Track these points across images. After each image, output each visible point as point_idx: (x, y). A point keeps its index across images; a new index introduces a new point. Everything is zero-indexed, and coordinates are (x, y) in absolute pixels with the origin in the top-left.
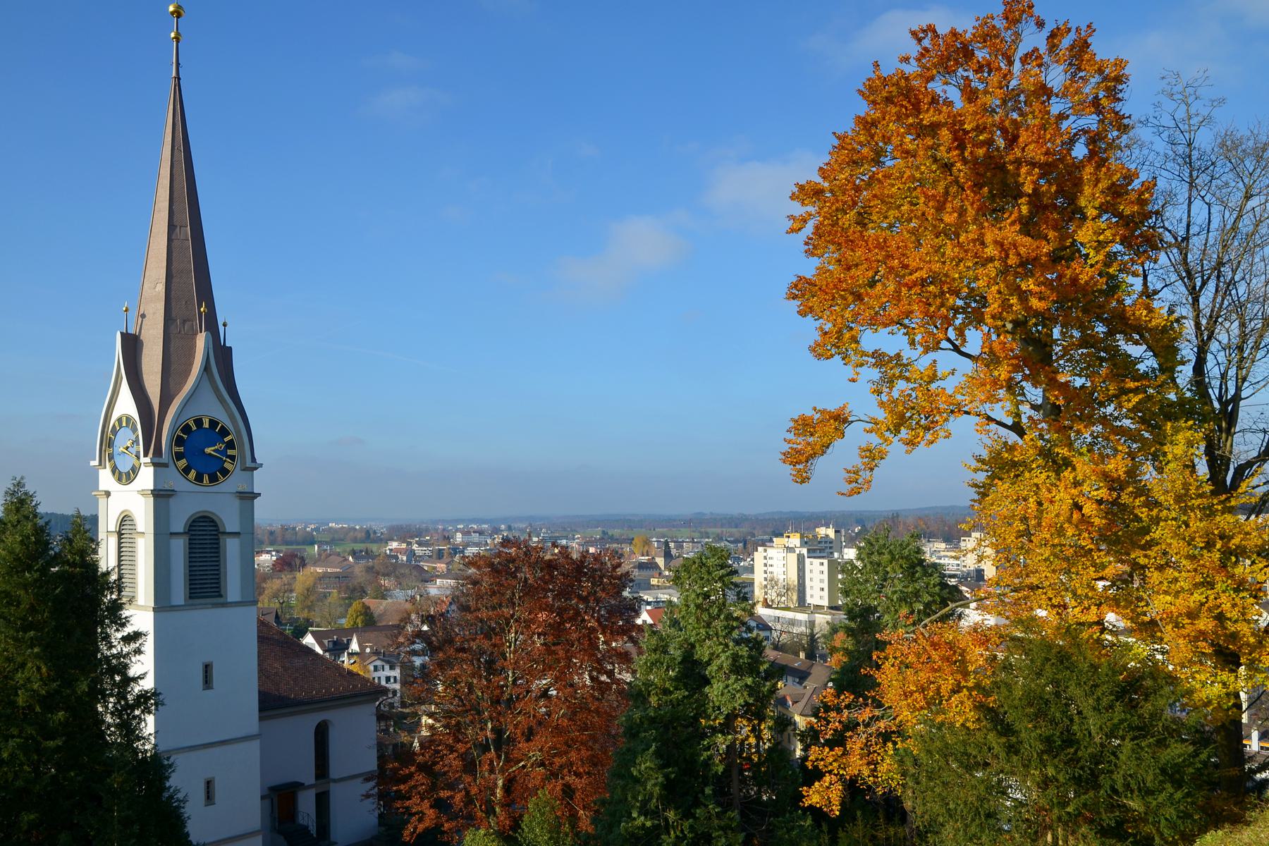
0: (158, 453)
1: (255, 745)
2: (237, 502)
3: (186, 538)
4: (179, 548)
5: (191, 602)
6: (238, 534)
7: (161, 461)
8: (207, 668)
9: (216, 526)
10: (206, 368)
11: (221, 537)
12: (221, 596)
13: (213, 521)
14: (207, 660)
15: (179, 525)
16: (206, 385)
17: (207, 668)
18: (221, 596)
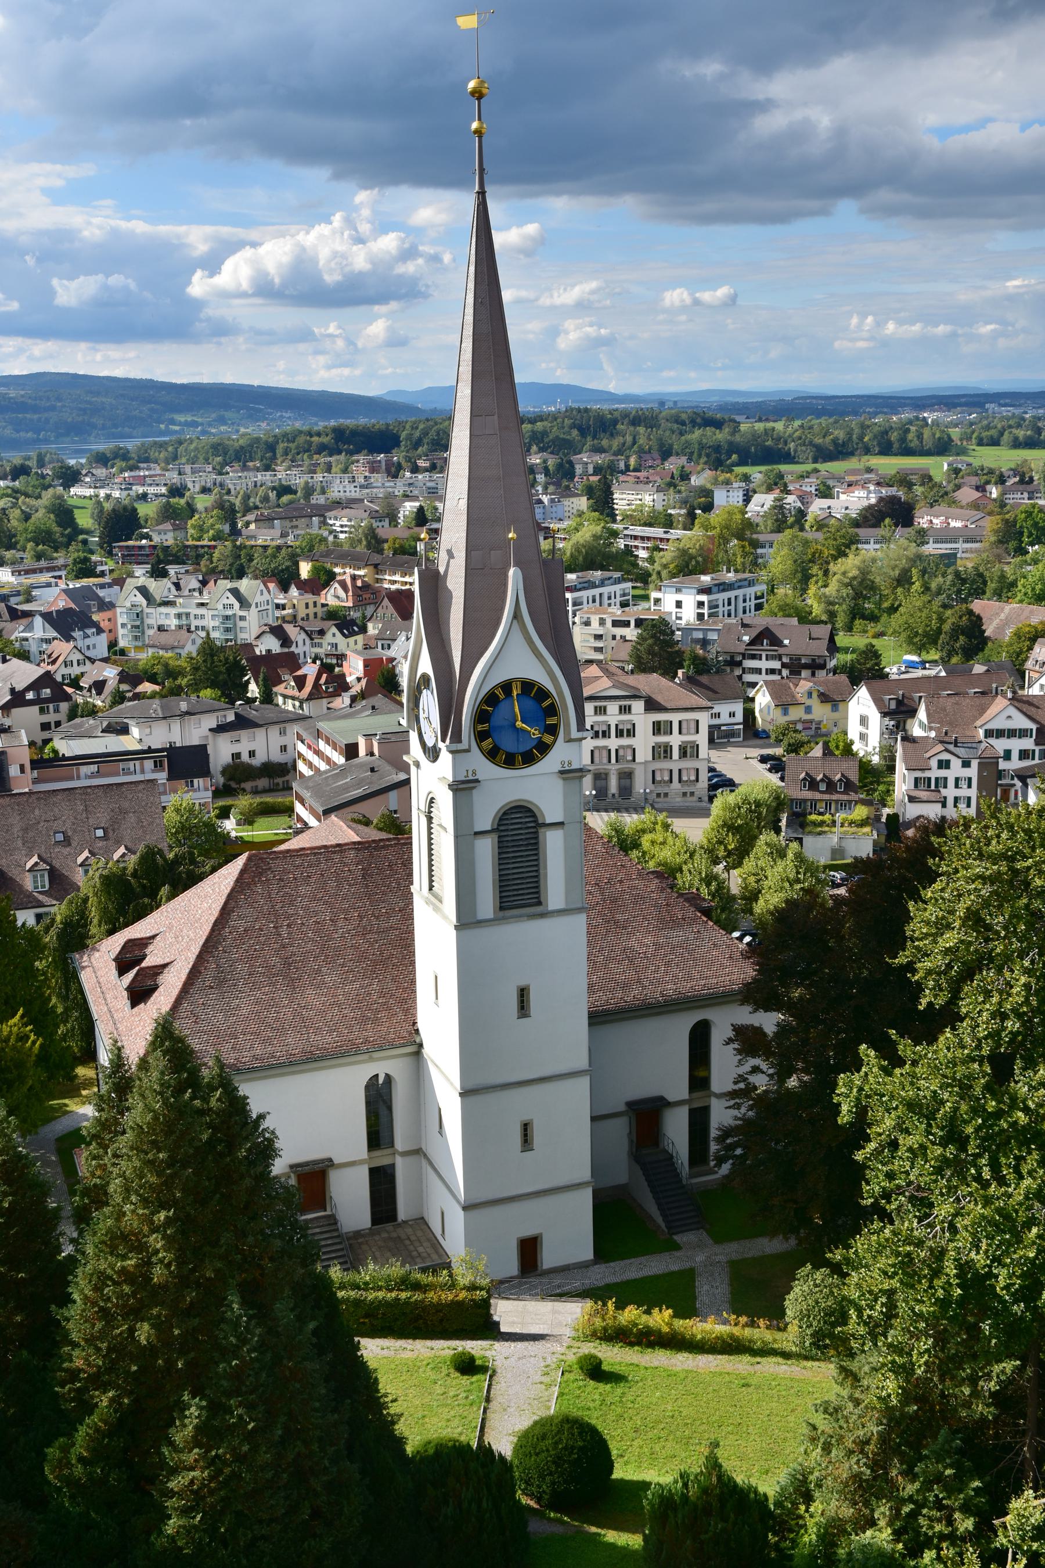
0: (457, 738)
1: (585, 1082)
2: (559, 783)
3: (495, 837)
4: (486, 850)
5: (501, 914)
6: (561, 824)
7: (460, 747)
8: (523, 993)
9: (534, 816)
10: (516, 615)
11: (541, 830)
12: (539, 903)
13: (530, 810)
14: (523, 983)
15: (485, 820)
16: (517, 636)
17: (523, 993)
18: (539, 903)
